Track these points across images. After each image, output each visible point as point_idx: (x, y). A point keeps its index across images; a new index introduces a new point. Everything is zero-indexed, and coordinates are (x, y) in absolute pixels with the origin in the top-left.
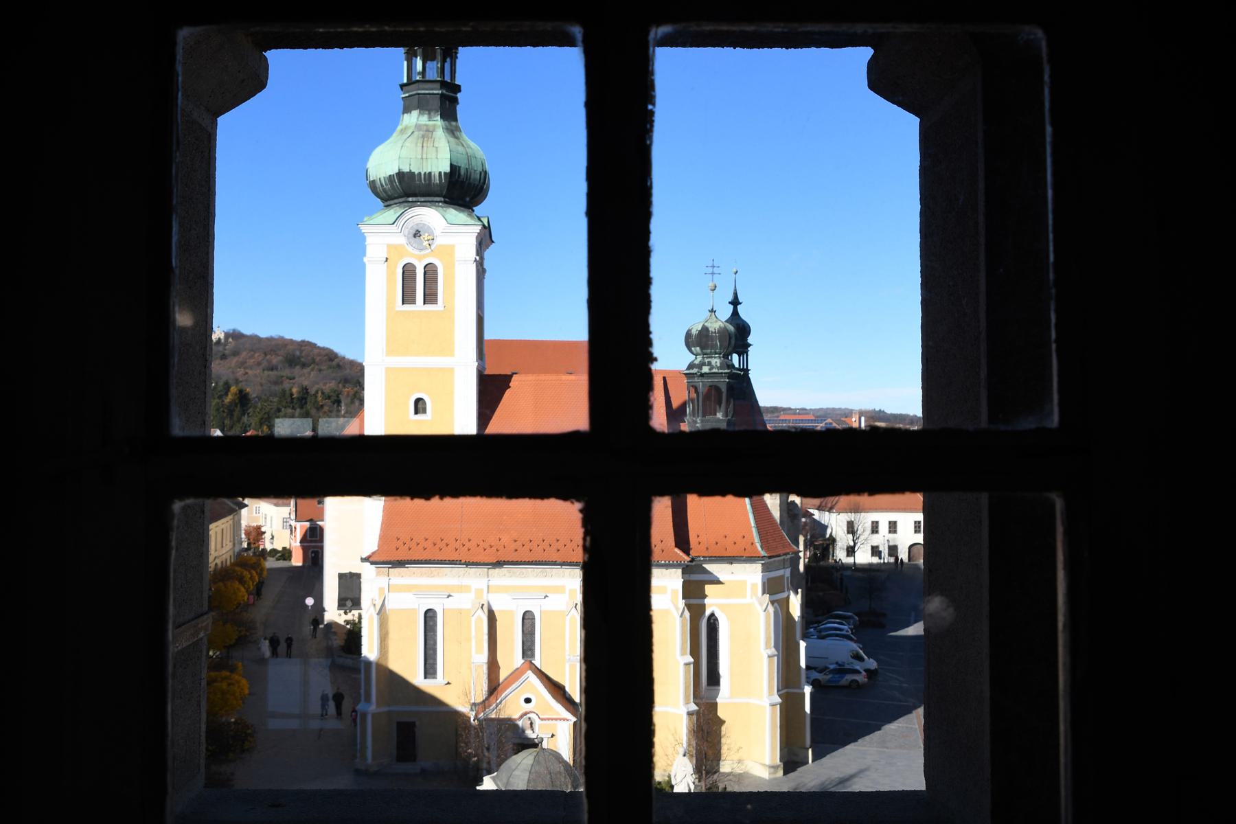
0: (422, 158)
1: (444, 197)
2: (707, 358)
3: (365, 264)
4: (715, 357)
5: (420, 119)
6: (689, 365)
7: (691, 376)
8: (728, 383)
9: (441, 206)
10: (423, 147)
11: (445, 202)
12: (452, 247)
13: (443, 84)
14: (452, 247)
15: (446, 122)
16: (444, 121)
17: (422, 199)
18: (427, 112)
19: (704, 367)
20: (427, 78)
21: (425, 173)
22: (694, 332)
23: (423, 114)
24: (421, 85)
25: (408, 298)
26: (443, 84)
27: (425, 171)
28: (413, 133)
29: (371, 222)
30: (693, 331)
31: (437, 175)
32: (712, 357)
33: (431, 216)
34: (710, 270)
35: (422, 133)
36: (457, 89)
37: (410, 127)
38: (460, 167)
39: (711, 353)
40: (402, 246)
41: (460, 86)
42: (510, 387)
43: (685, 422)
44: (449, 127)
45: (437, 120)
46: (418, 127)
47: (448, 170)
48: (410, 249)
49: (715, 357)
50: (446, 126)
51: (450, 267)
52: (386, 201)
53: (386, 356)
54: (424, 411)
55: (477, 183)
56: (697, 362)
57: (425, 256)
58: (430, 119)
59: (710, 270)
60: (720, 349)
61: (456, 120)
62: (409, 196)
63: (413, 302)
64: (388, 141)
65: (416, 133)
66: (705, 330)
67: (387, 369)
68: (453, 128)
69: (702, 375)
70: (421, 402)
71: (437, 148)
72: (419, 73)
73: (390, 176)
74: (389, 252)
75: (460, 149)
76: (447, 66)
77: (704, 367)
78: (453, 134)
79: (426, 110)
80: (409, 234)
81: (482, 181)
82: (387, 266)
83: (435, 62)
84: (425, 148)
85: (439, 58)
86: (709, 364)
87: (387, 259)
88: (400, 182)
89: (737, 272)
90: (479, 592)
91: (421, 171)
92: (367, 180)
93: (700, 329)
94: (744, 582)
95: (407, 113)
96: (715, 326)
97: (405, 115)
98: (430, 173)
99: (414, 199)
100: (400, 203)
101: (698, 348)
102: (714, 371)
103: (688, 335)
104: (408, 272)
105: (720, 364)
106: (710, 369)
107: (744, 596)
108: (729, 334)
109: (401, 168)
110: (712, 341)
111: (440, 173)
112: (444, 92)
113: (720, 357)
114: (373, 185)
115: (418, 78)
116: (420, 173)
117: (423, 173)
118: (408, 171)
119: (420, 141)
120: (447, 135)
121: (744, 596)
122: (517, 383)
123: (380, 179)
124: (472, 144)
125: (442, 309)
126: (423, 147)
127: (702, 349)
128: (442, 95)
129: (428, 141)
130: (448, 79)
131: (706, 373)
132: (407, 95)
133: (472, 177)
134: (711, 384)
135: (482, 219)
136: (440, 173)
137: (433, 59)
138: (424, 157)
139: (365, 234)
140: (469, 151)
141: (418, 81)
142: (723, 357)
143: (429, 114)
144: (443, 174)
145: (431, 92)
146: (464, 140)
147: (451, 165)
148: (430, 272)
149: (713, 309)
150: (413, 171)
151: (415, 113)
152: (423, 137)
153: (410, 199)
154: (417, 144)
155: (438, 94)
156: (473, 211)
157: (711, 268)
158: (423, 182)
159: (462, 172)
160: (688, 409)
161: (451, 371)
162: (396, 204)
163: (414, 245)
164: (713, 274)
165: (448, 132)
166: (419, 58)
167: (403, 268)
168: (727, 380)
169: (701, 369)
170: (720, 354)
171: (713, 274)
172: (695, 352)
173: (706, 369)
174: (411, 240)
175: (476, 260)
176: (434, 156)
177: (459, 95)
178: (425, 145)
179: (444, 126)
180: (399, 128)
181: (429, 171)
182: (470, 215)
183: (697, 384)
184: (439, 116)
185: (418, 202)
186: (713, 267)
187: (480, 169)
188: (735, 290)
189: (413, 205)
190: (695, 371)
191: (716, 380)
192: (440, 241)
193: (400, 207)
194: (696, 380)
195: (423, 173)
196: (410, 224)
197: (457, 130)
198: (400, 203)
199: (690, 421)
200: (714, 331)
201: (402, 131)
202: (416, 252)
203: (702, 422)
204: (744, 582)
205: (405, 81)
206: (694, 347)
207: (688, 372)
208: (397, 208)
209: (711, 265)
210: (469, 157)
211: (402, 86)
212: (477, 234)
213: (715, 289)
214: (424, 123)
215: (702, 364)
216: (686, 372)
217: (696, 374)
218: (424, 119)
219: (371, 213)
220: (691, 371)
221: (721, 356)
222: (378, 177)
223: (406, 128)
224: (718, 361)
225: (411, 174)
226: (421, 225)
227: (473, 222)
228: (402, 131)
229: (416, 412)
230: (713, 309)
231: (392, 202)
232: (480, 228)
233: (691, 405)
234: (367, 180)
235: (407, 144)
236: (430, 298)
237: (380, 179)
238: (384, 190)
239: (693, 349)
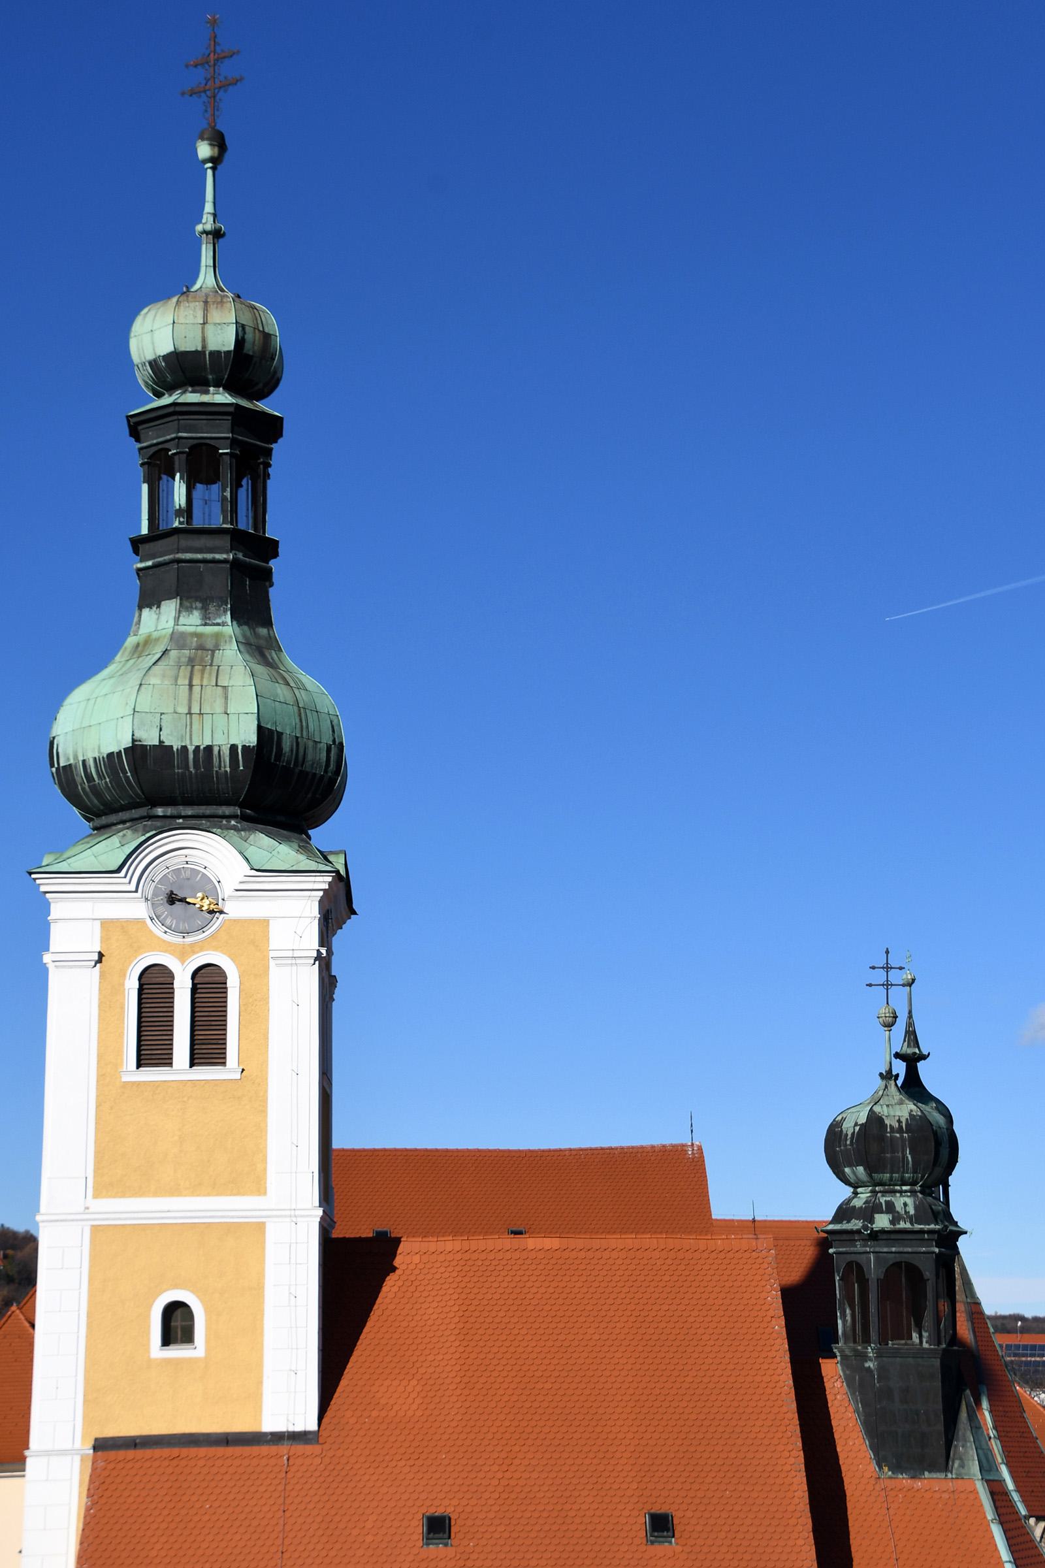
0: (190, 713)
1: (241, 806)
2: (884, 1193)
3: (47, 970)
4: (901, 1192)
5: (181, 618)
6: (840, 1208)
7: (845, 1237)
8: (938, 1256)
9: (235, 828)
10: (191, 686)
11: (244, 818)
12: (264, 923)
13: (238, 538)
14: (264, 923)
15: (246, 628)
16: (240, 625)
17: (189, 811)
18: (199, 605)
19: (876, 1216)
20: (197, 523)
21: (198, 747)
22: (848, 1127)
23: (190, 609)
24: (185, 541)
26: (238, 538)
28: (165, 652)
29: (63, 867)
30: (844, 1126)
31: (226, 752)
32: (895, 1192)
34: (880, 976)
35: (187, 652)
36: (270, 549)
37: (157, 640)
38: (280, 734)
39: (892, 1182)
40: (139, 922)
41: (274, 544)
42: (394, 1269)
43: (835, 1357)
44: (253, 640)
45: (223, 624)
46: (178, 639)
47: (252, 739)
48: (157, 930)
49: (901, 1192)
50: (244, 636)
51: (257, 974)
52: (98, 816)
53: (95, 1196)
56: (858, 1203)
57: (194, 949)
58: (206, 621)
59: (880, 976)
60: (915, 1172)
61: (268, 623)
62: (155, 804)
63: (164, 1059)
64: (105, 673)
65: (173, 654)
66: (875, 1120)
67: (96, 1230)
68: (262, 643)
69: (875, 1236)
70: (179, 1313)
71: (224, 687)
72: (179, 512)
73: (110, 755)
74: (104, 939)
75: (282, 691)
76: (244, 494)
77: (876, 1216)
78: (263, 655)
79: (197, 599)
80: (155, 895)
81: (332, 766)
82: (102, 975)
83: (215, 488)
84: (197, 689)
85: (227, 475)
86: (890, 1208)
87: (101, 955)
88: (135, 771)
89: (913, 980)
91: (187, 743)
92: (52, 765)
93: (863, 1120)
95: (150, 606)
96: (898, 1113)
97: (146, 612)
98: (209, 748)
99: (169, 811)
100: (132, 820)
101: (861, 1169)
102: (902, 1225)
103: (834, 1135)
105: (916, 1208)
106: (892, 1222)
108: (935, 1133)
109: (137, 736)
110: (893, 1152)
111: (233, 748)
112: (240, 556)
113: (913, 1192)
114: (66, 778)
115: (176, 524)
116: (185, 748)
117: (191, 749)
118: (157, 743)
119: (185, 672)
120: (248, 657)
122: (416, 1259)
123: (84, 761)
124: (308, 680)
125: (238, 1076)
126: (191, 686)
127: (870, 1170)
128: (235, 563)
129: (203, 672)
130: (245, 523)
131: (883, 1231)
132: (150, 563)
133: (309, 757)
134: (899, 1258)
135: (331, 858)
136: (233, 748)
137: (210, 481)
138: (195, 710)
139: (50, 900)
140: (302, 696)
141: (176, 531)
142: (921, 1192)
143: (205, 609)
144: (240, 748)
145: (209, 556)
146: (288, 671)
147: (260, 729)
149: (890, 1071)
150: (167, 743)
151: (170, 607)
152: (191, 662)
153: (160, 811)
154: (176, 679)
155: (225, 561)
156: (309, 837)
157: (883, 972)
158: (192, 769)
159: (287, 745)
160: (840, 1322)
161: (259, 1228)
162: (124, 822)
163: (168, 922)
164: (887, 985)
165: (252, 655)
166: (178, 475)
167: (140, 978)
168: (937, 1250)
169: (872, 1221)
170: (914, 1184)
171: (887, 985)
172: (852, 1179)
173: (882, 1221)
174: (160, 909)
176: (219, 708)
177: (273, 564)
178: (196, 681)
179: (241, 639)
180: (131, 641)
181: (207, 742)
182: (305, 847)
183: (861, 1259)
184: (228, 618)
185: (180, 817)
186: (887, 968)
187: (327, 739)
188: (910, 1024)
189: (168, 824)
190: (856, 1224)
191: (910, 1250)
192: (235, 909)
193: (136, 831)
194: (859, 1247)
195: (191, 749)
196: (159, 871)
197: (270, 647)
198: (132, 820)
199: (848, 1352)
200: (896, 1125)
201: (139, 649)
202: (176, 939)
203: (879, 1355)
205: (145, 530)
206: (850, 1165)
207: (837, 1227)
208: (129, 833)
209: (882, 963)
210: (301, 711)
211: (137, 544)
212: (321, 893)
213: (893, 1025)
214: (191, 629)
215: (872, 1209)
216: (831, 1227)
217: (858, 1232)
218: (192, 622)
219: (60, 848)
220: (845, 1226)
221: (918, 1188)
222: (81, 758)
223: (148, 642)
224: (910, 1201)
226: (188, 873)
227: (313, 865)
228: (139, 649)
229: (167, 1341)
230: (890, 1071)
231: (113, 818)
232: (330, 879)
233: (848, 1311)
234: (52, 765)
235: (154, 680)
237: (84, 761)
238: (95, 790)
239: (847, 1170)
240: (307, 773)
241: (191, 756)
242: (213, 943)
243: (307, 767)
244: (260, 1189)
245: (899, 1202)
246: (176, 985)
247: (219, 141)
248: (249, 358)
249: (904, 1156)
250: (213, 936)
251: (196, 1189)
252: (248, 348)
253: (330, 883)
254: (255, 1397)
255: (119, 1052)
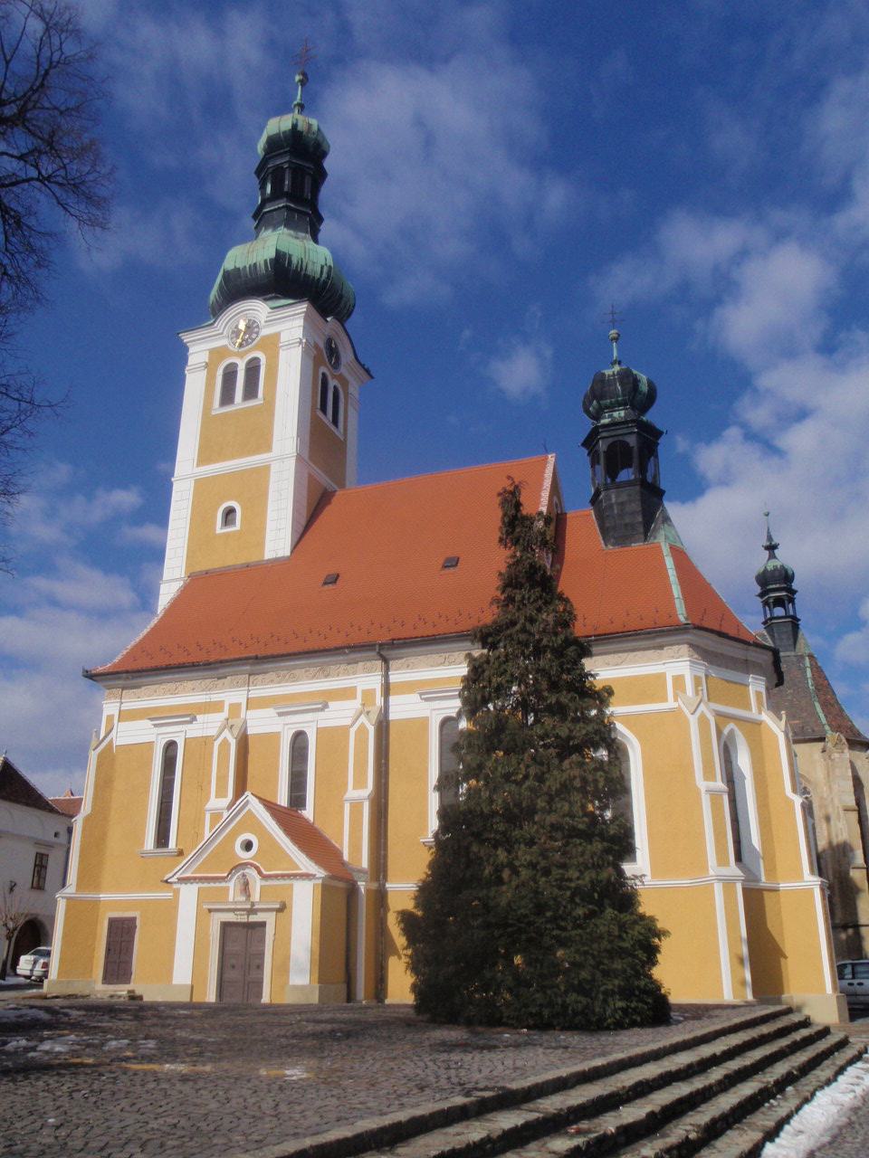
12: (278, 335)
14: (278, 335)
21: (250, 266)
25: (227, 398)
27: (250, 263)
31: (262, 263)
33: (258, 309)
38: (290, 256)
40: (225, 346)
47: (273, 255)
54: (233, 522)
55: (318, 276)
81: (325, 275)
90: (235, 708)
94: (662, 677)
104: (230, 375)
107: (665, 699)
111: (266, 261)
116: (245, 267)
117: (248, 266)
121: (665, 699)
133: (310, 267)
134: (616, 439)
147: (278, 252)
148: (253, 369)
159: (295, 261)
175: (301, 342)
188: (768, 532)
204: (662, 677)
224: (622, 413)
225: (237, 270)
236: (251, 391)
240: (309, 276)
241: (248, 269)
242: (256, 348)
243: (309, 272)
244: (269, 448)
245: (616, 414)
246: (238, 369)
247: (304, 74)
248: (302, 133)
249: (616, 387)
250: (256, 345)
251: (242, 453)
252: (299, 128)
253: (307, 308)
254: (261, 545)
255: (211, 403)
